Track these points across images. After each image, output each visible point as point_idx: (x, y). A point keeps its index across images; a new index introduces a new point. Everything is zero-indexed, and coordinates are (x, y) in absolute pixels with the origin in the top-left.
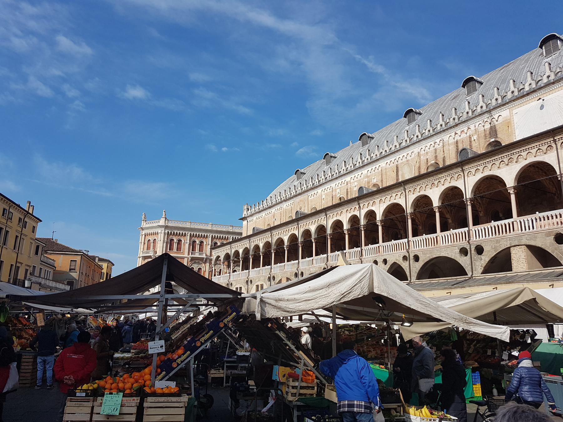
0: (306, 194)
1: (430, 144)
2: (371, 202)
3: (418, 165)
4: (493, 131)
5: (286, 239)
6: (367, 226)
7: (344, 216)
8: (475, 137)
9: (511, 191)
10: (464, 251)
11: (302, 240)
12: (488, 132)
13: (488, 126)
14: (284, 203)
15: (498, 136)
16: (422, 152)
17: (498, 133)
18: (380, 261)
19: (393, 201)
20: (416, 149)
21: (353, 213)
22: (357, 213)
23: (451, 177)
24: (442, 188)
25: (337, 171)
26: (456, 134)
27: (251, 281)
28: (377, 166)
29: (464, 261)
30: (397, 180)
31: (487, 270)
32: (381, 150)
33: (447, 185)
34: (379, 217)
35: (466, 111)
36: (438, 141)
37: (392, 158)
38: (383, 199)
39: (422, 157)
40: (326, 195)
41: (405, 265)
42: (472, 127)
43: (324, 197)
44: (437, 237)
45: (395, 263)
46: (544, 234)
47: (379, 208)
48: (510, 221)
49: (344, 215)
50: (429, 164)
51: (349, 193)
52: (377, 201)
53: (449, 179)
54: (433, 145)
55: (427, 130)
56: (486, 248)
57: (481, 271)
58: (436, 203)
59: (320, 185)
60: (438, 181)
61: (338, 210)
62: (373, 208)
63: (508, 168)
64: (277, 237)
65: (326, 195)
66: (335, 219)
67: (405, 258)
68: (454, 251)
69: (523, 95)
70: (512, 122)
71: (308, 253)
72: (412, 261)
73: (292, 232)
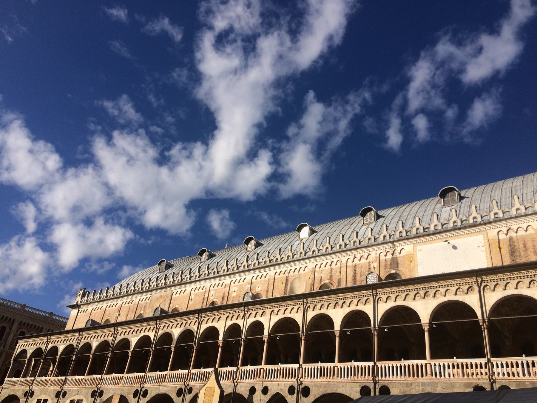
0: (170, 289)
1: (326, 262)
2: (260, 312)
3: (310, 281)
4: (395, 262)
5: (134, 341)
6: (248, 342)
7: (222, 325)
8: (376, 265)
9: (426, 328)
12: (389, 263)
13: (389, 256)
14: (138, 295)
15: (401, 268)
16: (317, 269)
17: (399, 265)
18: (259, 389)
19: (288, 315)
20: (310, 264)
21: (234, 321)
22: (240, 322)
23: (358, 299)
24: (347, 310)
25: (215, 270)
26: (355, 257)
28: (265, 274)
30: (285, 293)
32: (273, 258)
33: (353, 307)
35: (369, 237)
36: (335, 261)
37: (283, 268)
38: (276, 310)
39: (316, 274)
40: (196, 295)
42: (373, 254)
43: (192, 297)
44: (334, 367)
45: (278, 394)
46: (462, 384)
47: (269, 320)
48: (423, 362)
49: (222, 322)
50: (323, 283)
51: (226, 298)
52: (268, 312)
53: (355, 301)
54: (330, 263)
55: (325, 248)
58: (337, 327)
59: (192, 282)
60: (343, 301)
61: (216, 314)
62: (262, 319)
63: (423, 301)
64: (122, 337)
65: (196, 295)
66: (210, 324)
67: (291, 390)
68: (354, 389)
69: (427, 234)
70: (416, 258)
71: (160, 365)
72: (300, 395)
73: (146, 333)
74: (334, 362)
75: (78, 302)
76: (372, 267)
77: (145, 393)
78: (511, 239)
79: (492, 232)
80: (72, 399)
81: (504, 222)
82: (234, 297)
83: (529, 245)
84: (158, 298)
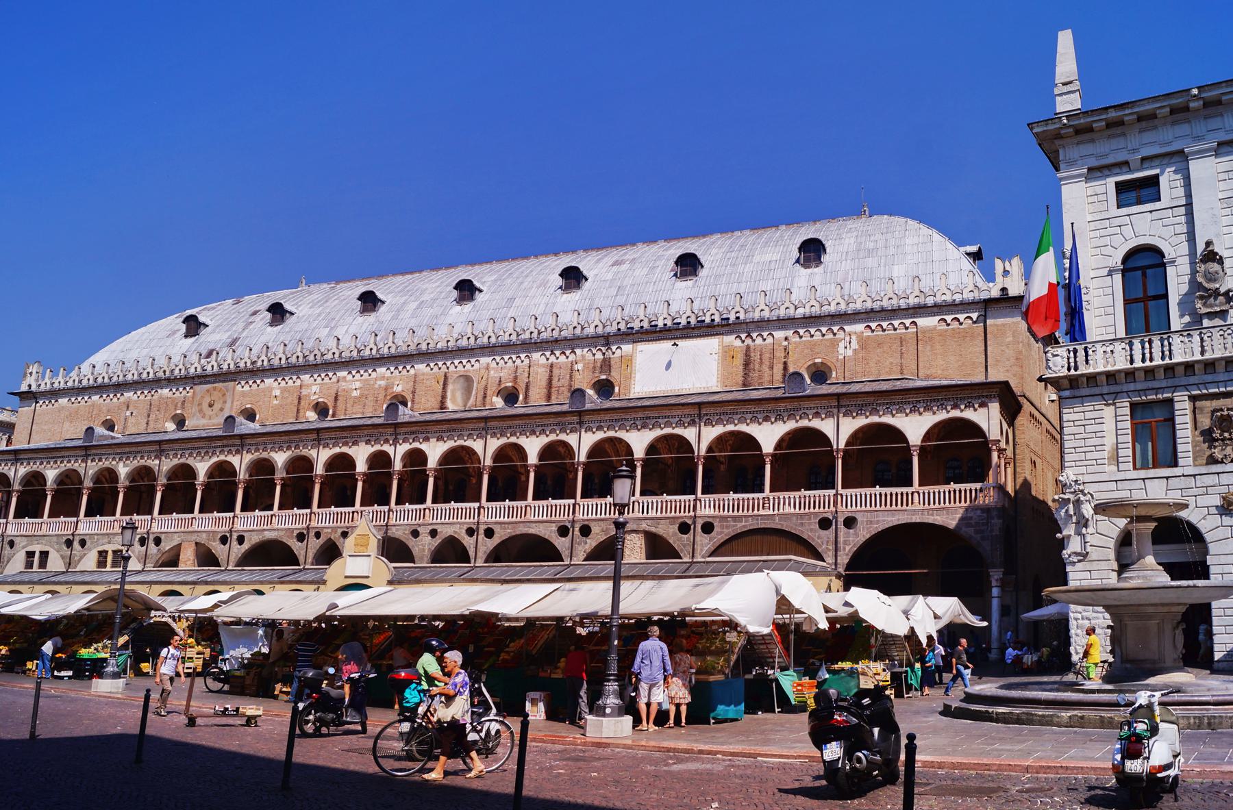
3: (483, 382)
4: (606, 365)
10: (563, 531)
11: (247, 477)
13: (599, 356)
15: (613, 374)
18: (425, 531)
27: (83, 543)
29: (561, 543)
31: (592, 556)
34: (432, 463)
41: (469, 542)
51: (340, 399)
56: (595, 529)
57: (582, 558)
62: (424, 447)
65: (283, 390)
72: (482, 536)
74: (526, 499)
75: (30, 386)
76: (576, 367)
77: (241, 540)
78: (748, 347)
79: (730, 339)
80: (101, 548)
81: (744, 326)
82: (355, 397)
83: (767, 356)
84: (208, 391)
